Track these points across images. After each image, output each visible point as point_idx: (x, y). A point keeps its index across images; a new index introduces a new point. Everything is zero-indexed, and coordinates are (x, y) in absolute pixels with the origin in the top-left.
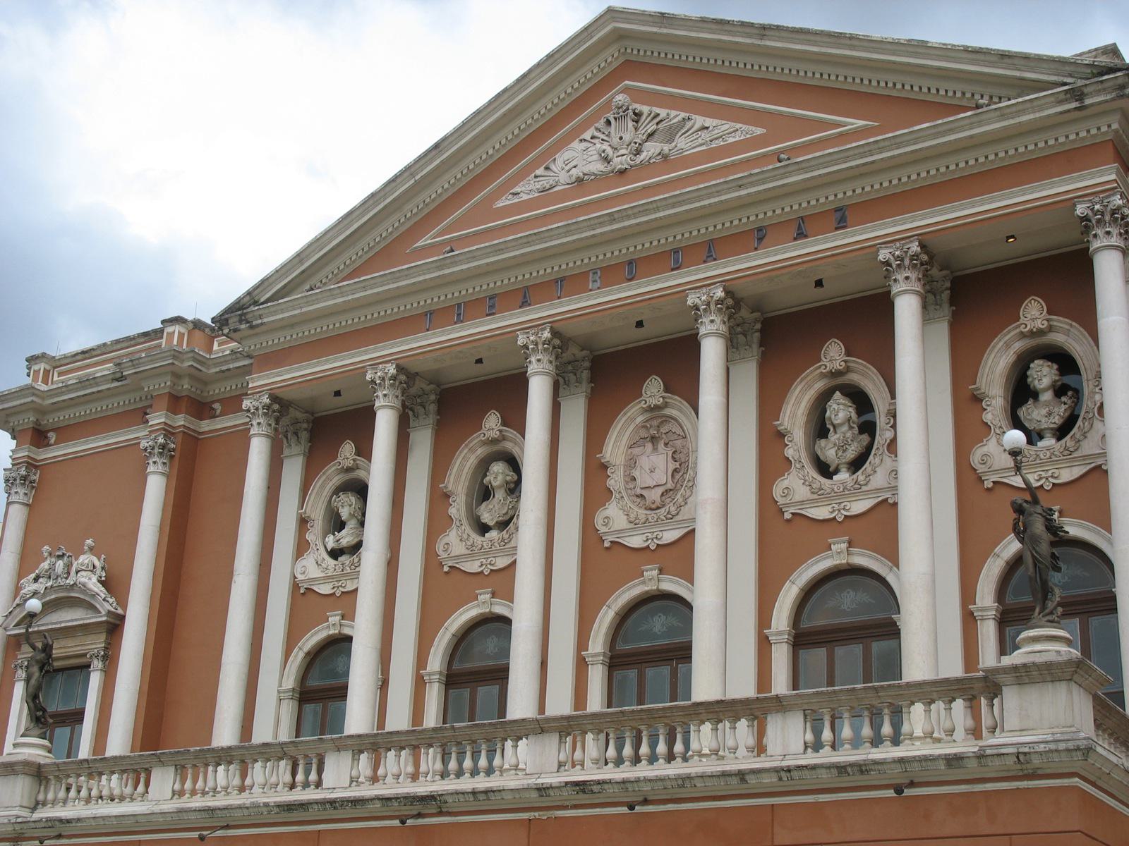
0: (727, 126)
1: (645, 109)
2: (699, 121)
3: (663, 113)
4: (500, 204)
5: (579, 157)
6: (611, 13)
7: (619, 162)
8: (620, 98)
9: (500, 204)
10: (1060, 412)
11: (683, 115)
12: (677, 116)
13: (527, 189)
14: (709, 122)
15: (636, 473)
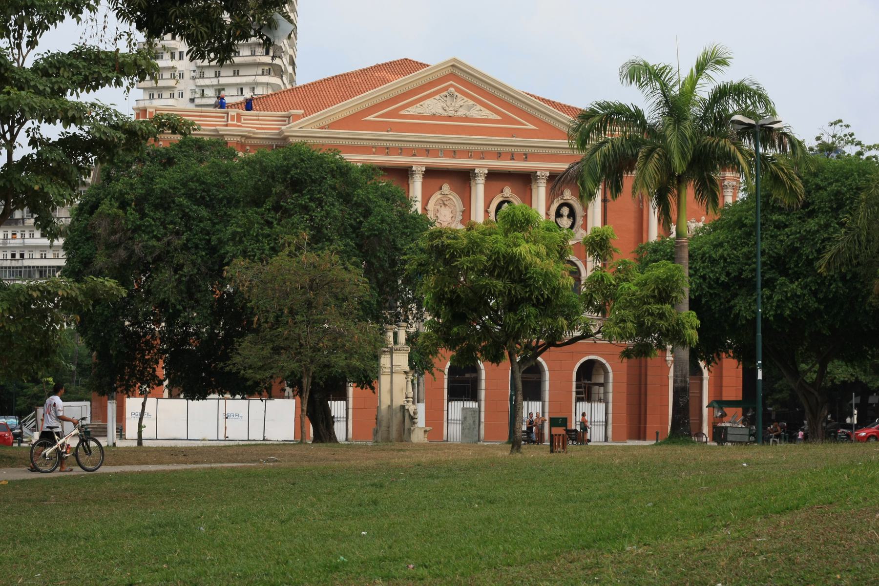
0: (488, 112)
1: (459, 95)
2: (479, 107)
3: (466, 99)
4: (402, 112)
5: (433, 106)
6: (455, 60)
7: (451, 113)
8: (452, 89)
9: (402, 112)
10: (570, 223)
11: (473, 102)
12: (471, 102)
13: (413, 110)
14: (482, 108)
15: (438, 215)
